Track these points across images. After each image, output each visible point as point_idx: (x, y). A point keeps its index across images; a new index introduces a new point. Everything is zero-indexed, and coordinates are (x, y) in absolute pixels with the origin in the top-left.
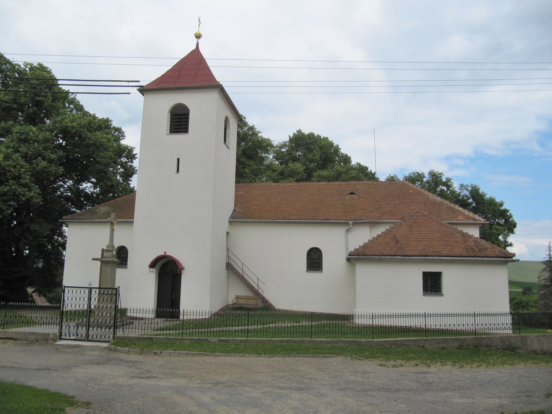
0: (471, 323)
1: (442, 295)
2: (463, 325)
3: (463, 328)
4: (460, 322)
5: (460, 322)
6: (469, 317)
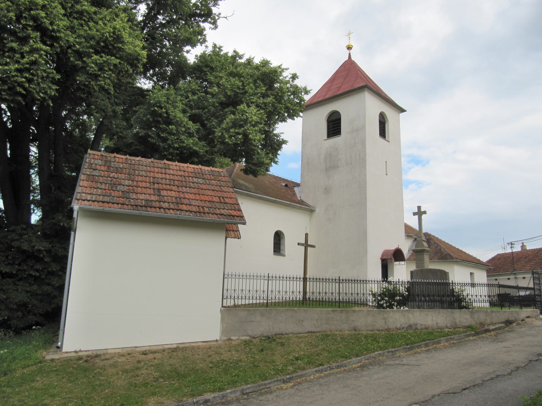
0: (262, 289)
1: (284, 255)
2: (358, 294)
3: (292, 297)
4: (347, 289)
5: (347, 289)
6: (259, 281)
